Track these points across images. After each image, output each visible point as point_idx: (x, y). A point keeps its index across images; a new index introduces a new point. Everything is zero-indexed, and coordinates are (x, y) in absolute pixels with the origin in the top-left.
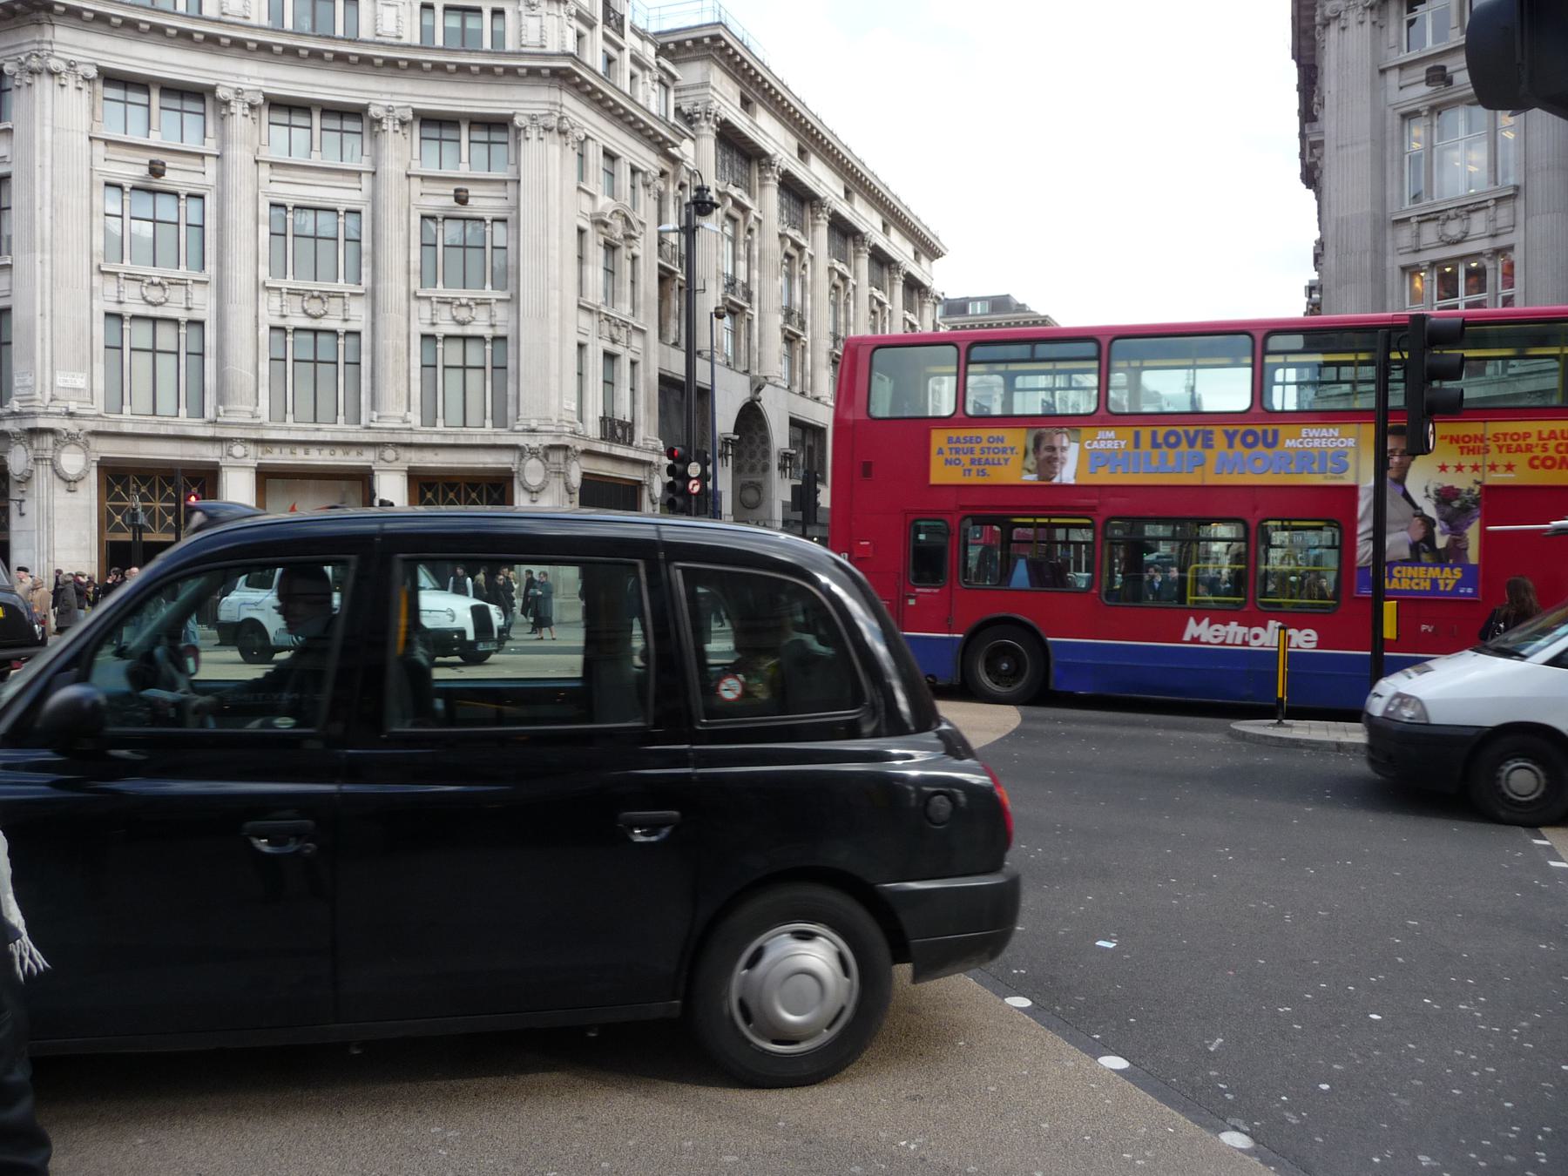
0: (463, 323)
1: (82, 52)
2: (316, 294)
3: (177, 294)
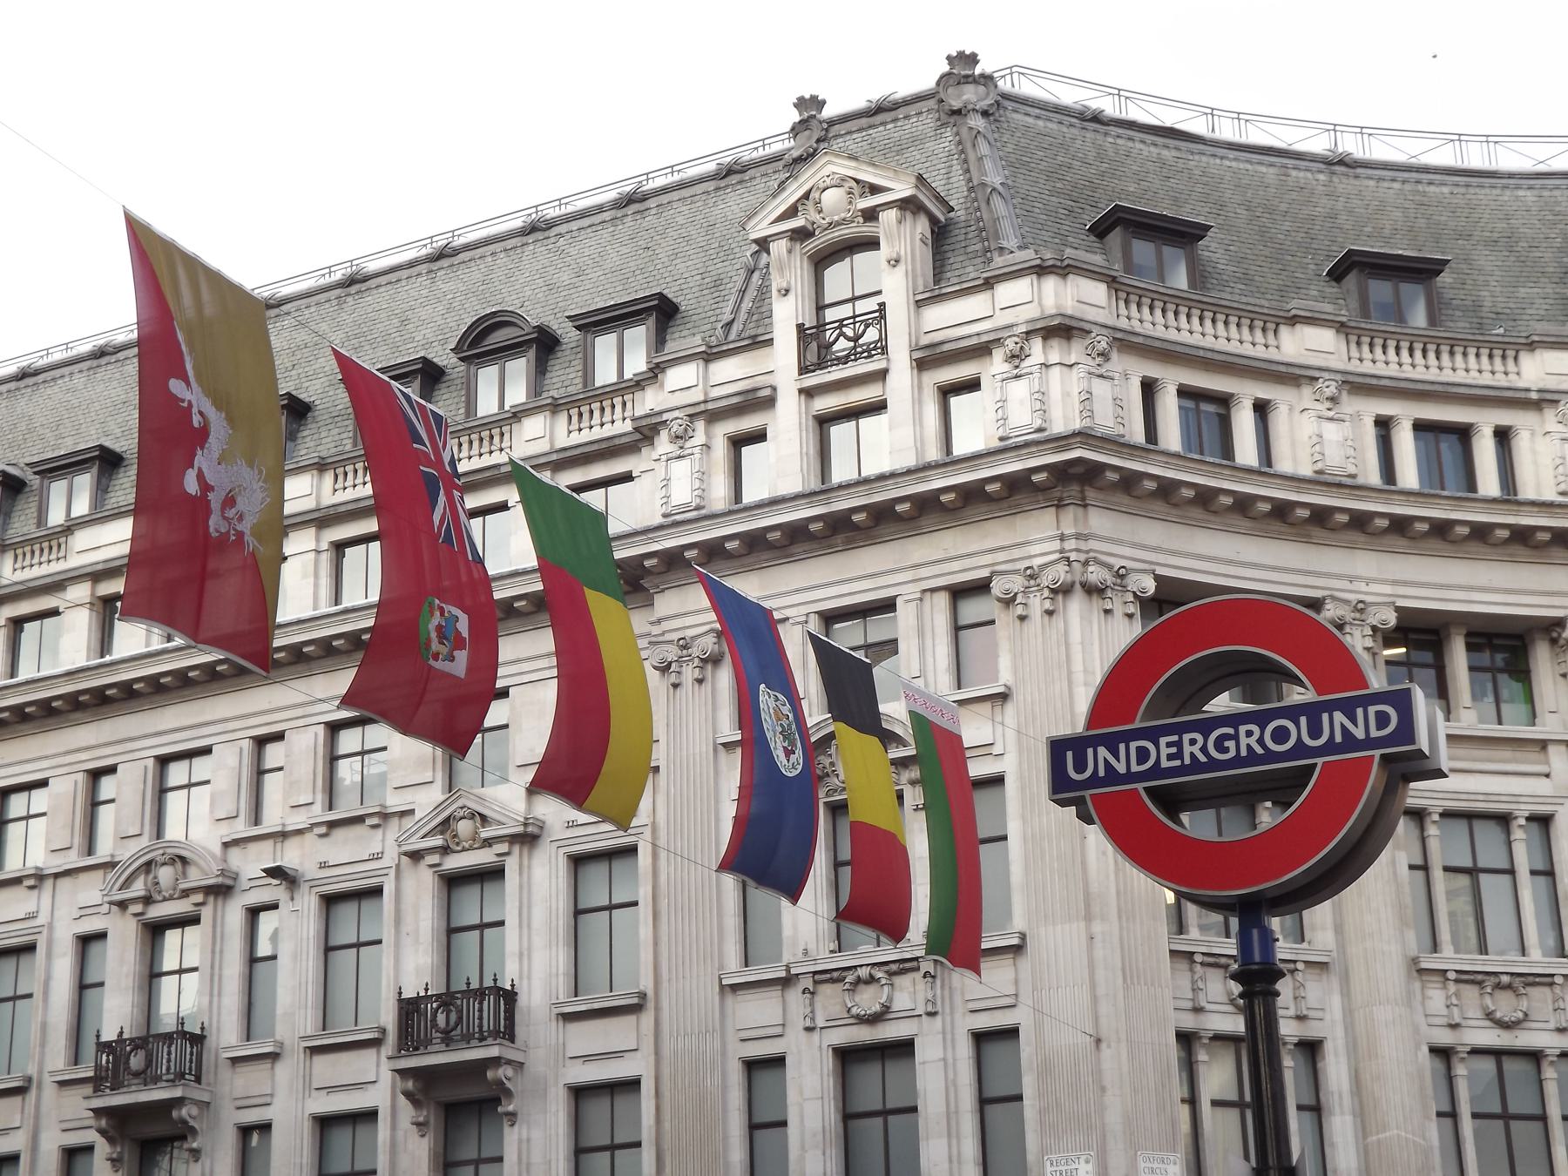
1: (1128, 551)
2: (1505, 979)
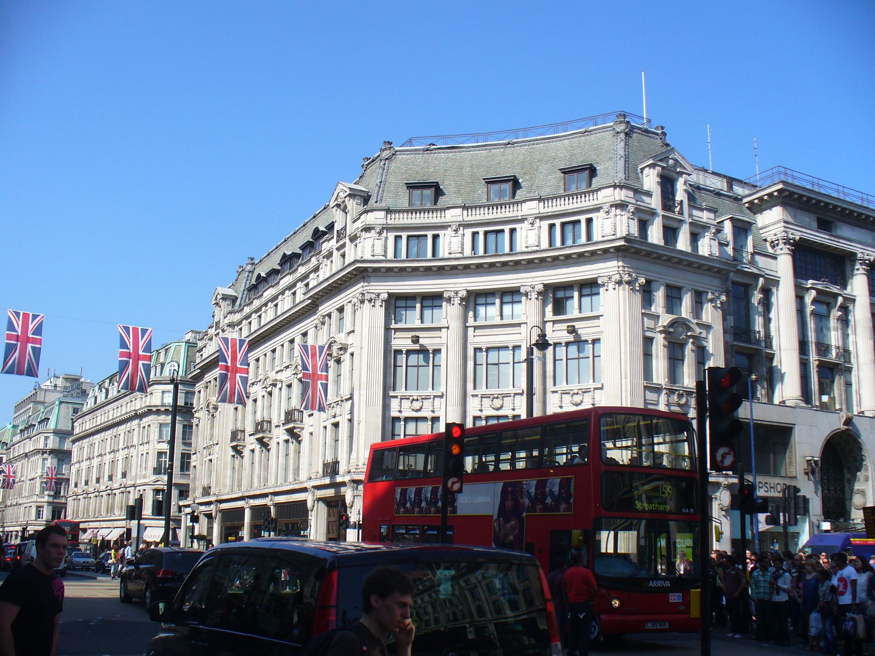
0: (577, 405)
2: (496, 396)
3: (427, 404)
